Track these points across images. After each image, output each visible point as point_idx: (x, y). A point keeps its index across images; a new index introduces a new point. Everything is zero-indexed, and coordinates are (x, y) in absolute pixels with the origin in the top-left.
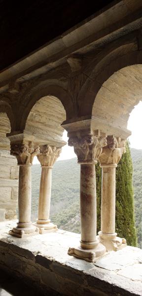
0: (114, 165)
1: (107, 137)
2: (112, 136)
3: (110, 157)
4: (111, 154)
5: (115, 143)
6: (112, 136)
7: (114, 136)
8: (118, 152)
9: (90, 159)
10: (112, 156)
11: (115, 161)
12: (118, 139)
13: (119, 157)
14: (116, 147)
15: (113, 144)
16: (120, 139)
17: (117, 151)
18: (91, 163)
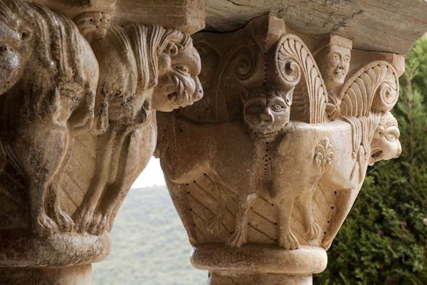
0: (291, 262)
1: (196, 22)
2: (261, 23)
3: (251, 198)
4: (255, 170)
5: (291, 81)
6: (261, 23)
7: (277, 28)
8: (322, 157)
9: (16, 221)
10: (269, 187)
11: (306, 225)
12: (320, 47)
13: (340, 195)
14: (301, 113)
15: (272, 85)
16: (341, 49)
17: (308, 147)
18: (23, 264)
